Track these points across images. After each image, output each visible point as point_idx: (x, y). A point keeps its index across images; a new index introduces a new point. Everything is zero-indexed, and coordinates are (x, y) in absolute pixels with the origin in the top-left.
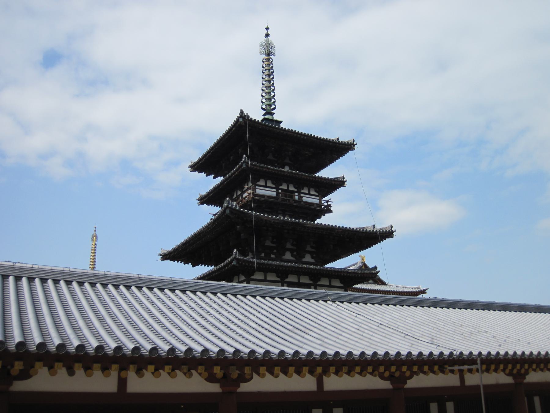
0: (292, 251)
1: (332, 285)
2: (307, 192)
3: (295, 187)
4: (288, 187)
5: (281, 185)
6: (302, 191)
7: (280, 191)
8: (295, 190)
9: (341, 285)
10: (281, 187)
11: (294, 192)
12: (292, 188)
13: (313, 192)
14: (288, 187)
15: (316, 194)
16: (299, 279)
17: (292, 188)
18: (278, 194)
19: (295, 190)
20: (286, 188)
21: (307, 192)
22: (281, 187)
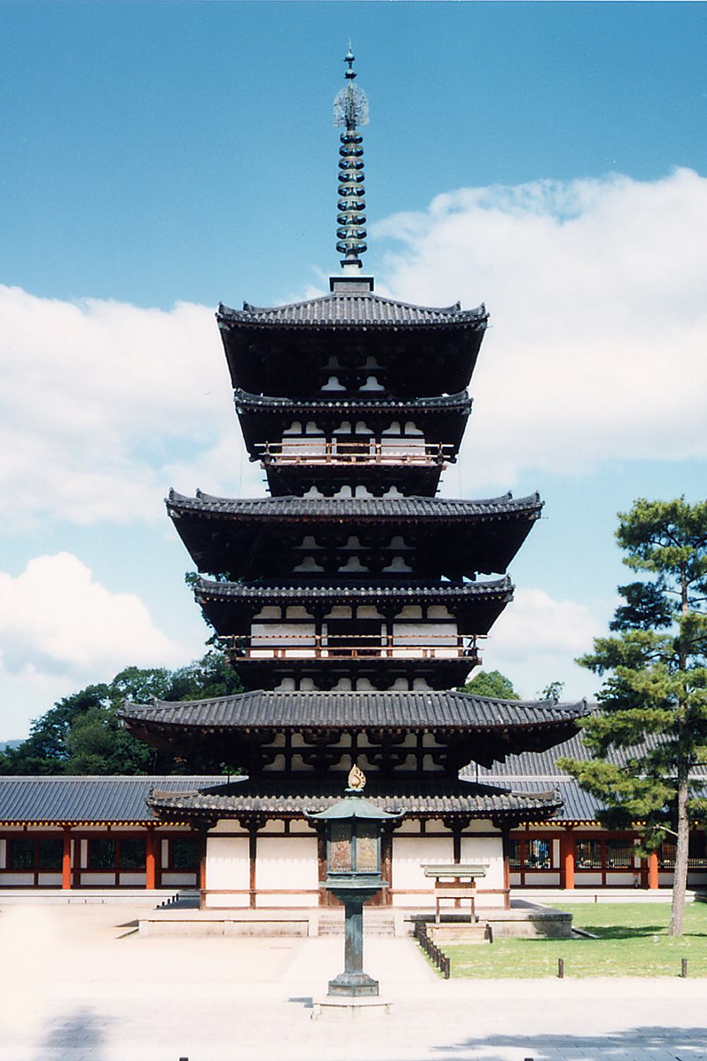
0: (361, 556)
1: (428, 617)
2: (398, 432)
3: (368, 427)
4: (353, 430)
5: (338, 427)
6: (385, 432)
7: (334, 440)
8: (370, 432)
9: (449, 617)
10: (336, 432)
11: (365, 438)
12: (362, 430)
13: (410, 430)
14: (353, 430)
15: (420, 433)
16: (354, 614)
17: (362, 430)
18: (329, 449)
19: (370, 432)
20: (349, 432)
21: (398, 432)
22: (336, 432)
